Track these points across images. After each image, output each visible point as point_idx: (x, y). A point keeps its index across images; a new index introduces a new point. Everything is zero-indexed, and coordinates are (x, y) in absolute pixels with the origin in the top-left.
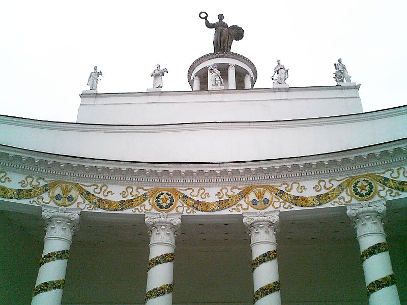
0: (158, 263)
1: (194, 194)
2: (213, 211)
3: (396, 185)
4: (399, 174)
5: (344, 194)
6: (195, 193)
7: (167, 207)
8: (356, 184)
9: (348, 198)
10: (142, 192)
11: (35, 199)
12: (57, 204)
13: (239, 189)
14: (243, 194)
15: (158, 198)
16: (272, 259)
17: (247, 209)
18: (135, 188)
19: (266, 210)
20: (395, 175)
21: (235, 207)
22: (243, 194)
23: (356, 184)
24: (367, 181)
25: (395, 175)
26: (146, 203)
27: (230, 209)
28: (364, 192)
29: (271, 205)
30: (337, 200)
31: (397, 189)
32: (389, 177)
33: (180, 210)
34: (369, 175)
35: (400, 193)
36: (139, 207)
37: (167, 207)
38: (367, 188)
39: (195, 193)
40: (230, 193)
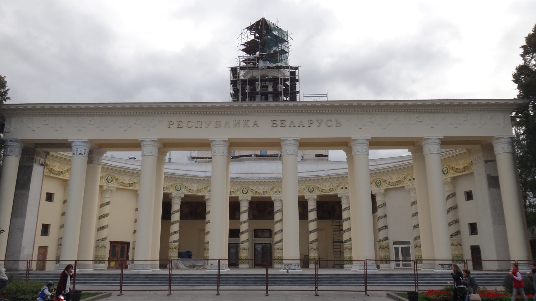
0: (244, 213)
1: (255, 189)
2: (262, 195)
3: (321, 190)
4: (322, 186)
5: (305, 191)
6: (255, 188)
7: (246, 193)
8: (309, 188)
9: (306, 193)
10: (237, 188)
11: (202, 193)
12: (209, 194)
13: (271, 187)
14: (272, 189)
15: (242, 190)
16: (281, 211)
17: (273, 194)
18: (234, 186)
19: (279, 195)
20: (321, 186)
21: (269, 194)
22: (272, 189)
23: (309, 188)
24: (313, 187)
25: (321, 186)
26: (239, 192)
27: (267, 194)
28: (311, 191)
29: (281, 194)
30: (302, 193)
31: (321, 191)
32: (320, 187)
33: (250, 194)
34: (313, 185)
35: (322, 193)
36: (236, 194)
37: (246, 193)
38: (312, 190)
39: (255, 188)
40: (267, 189)
